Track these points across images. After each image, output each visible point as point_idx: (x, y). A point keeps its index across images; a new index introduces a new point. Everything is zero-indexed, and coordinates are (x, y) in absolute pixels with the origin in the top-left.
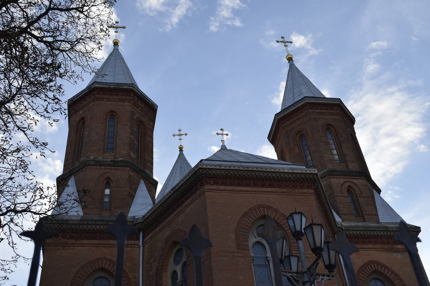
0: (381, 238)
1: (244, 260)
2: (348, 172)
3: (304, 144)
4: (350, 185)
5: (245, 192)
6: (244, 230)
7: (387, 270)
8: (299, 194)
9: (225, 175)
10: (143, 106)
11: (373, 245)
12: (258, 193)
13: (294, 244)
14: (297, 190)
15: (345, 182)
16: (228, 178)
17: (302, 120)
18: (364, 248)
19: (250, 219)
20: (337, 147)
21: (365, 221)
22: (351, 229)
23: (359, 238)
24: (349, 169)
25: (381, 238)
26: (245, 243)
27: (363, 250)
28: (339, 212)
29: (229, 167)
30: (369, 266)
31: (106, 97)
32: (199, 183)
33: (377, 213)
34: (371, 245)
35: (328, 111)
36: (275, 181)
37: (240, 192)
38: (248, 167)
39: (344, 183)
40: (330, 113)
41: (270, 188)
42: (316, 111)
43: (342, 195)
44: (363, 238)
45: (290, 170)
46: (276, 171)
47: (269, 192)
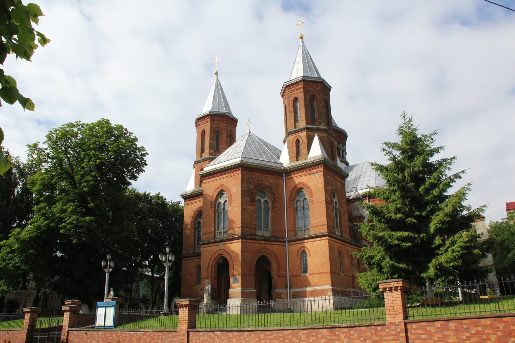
10: (218, 118)
31: (201, 122)
35: (297, 87)
39: (295, 138)
42: (291, 89)
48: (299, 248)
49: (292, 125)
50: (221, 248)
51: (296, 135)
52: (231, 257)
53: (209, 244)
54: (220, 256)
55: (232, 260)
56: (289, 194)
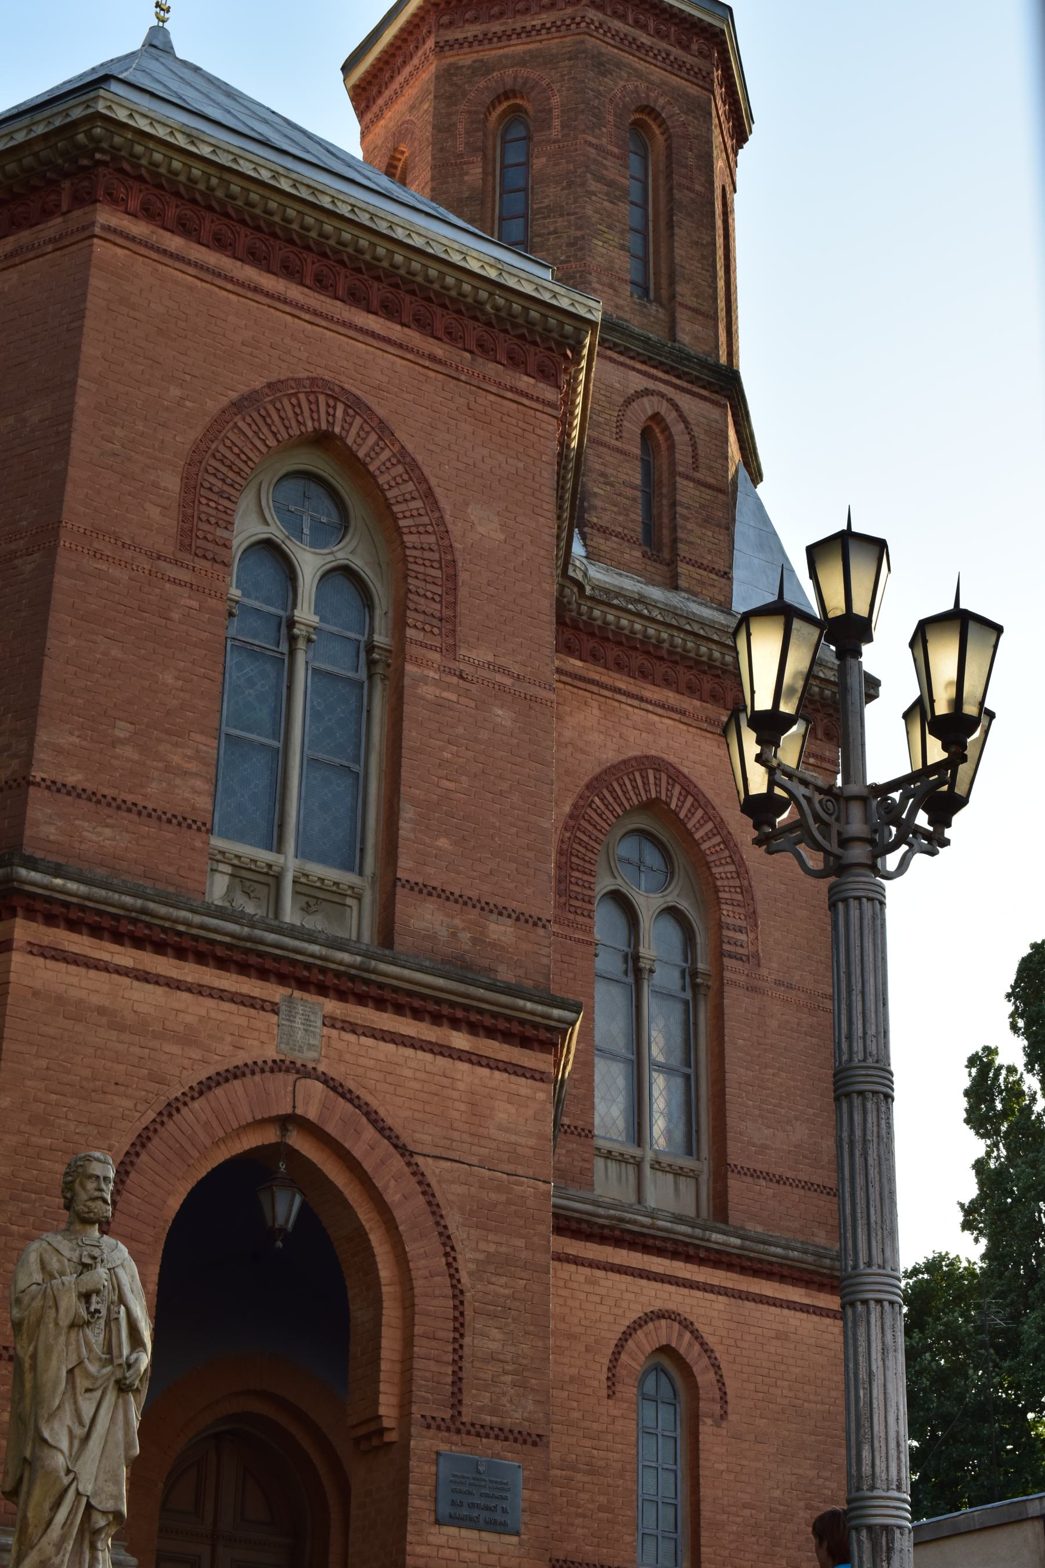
0: (718, 676)
1: (195, 604)
2: (671, 353)
3: (513, 158)
4: (663, 413)
5: (268, 301)
6: (224, 469)
7: (700, 813)
8: (494, 389)
9: (201, 186)
11: (678, 696)
12: (324, 323)
13: (422, 600)
14: (491, 369)
15: (647, 392)
16: (210, 208)
17: (537, 45)
18: (641, 699)
19: (265, 430)
20: (651, 224)
21: (676, 588)
22: (615, 602)
23: (635, 649)
24: (674, 341)
25: (718, 676)
26: (220, 532)
27: (636, 703)
28: (586, 516)
29: (231, 157)
30: (637, 775)
32: (66, 184)
33: (731, 567)
34: (671, 694)
35: (664, 45)
36: (412, 292)
37: (250, 294)
38: (314, 190)
40: (672, 58)
41: (381, 320)
42: (617, 24)
43: (618, 444)
44: (648, 653)
45: (491, 266)
46: (430, 251)
47: (373, 335)
48: (635, 1316)
49: (611, 286)
50: (307, 1056)
51: (651, 385)
52: (434, 1207)
53: (138, 943)
54: (270, 1136)
55: (446, 1238)
56: (567, 809)
